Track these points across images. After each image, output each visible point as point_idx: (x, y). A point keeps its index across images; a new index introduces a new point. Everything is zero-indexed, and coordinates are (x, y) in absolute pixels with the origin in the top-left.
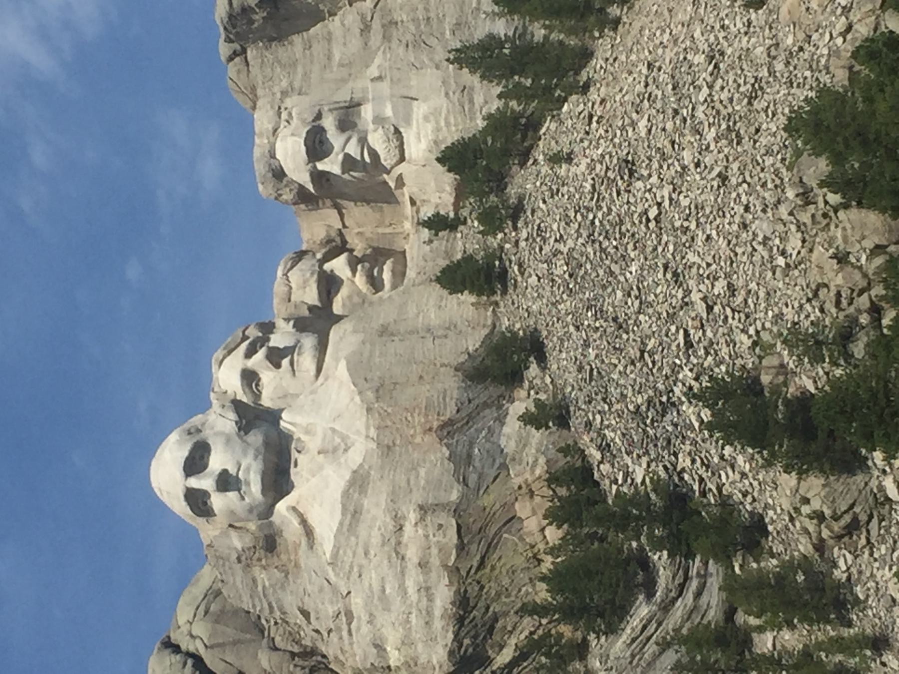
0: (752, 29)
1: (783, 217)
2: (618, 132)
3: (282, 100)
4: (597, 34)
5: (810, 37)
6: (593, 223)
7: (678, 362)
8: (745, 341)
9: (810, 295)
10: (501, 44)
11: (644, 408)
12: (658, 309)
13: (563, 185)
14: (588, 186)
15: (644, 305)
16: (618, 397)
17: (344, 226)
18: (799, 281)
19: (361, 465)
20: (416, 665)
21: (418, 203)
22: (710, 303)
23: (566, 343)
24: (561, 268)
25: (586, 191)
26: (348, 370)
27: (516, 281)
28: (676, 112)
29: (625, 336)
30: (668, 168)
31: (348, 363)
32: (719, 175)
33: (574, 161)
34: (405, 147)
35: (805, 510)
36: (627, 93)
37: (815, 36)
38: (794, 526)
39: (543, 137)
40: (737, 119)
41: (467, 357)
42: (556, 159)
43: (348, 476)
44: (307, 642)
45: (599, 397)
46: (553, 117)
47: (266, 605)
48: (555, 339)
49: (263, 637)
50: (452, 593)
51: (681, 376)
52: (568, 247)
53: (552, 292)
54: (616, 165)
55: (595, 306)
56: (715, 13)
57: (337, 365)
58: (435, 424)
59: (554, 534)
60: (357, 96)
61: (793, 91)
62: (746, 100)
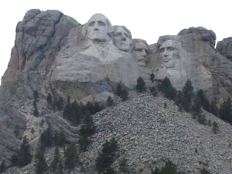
0: (191, 150)
1: (150, 157)
2: (170, 119)
3: (181, 41)
4: (192, 113)
5: (189, 163)
6: (151, 113)
7: (121, 132)
8: (125, 149)
9: (134, 163)
10: (191, 91)
11: (111, 125)
12: (132, 128)
13: (160, 106)
14: (159, 112)
15: (133, 125)
16: (114, 119)
17: (153, 54)
18: (137, 161)
19: (100, 61)
20: (57, 72)
21: (157, 71)
22: (133, 140)
23: (125, 107)
24: (142, 105)
25: (158, 112)
26: (121, 57)
27: (139, 95)
28: (174, 133)
29: (127, 120)
30: (162, 131)
31: (122, 57)
32: (160, 143)
33: (165, 109)
34: (170, 68)
35: (89, 161)
36: (179, 121)
37: (189, 164)
38: (86, 158)
39: (170, 101)
40: (172, 147)
41: (123, 83)
42: (165, 105)
43: (97, 57)
44: (62, 47)
45: (114, 114)
46: (175, 103)
47: (70, 38)
48: (126, 104)
49: (63, 37)
50: (72, 81)
51: (118, 133)
52: (146, 107)
53: (137, 103)
54: (163, 119)
55: (133, 114)
56: (195, 141)
57: (122, 54)
58: (109, 77)
59: (85, 103)
60: (181, 58)
61: (177, 160)
62: (176, 149)
